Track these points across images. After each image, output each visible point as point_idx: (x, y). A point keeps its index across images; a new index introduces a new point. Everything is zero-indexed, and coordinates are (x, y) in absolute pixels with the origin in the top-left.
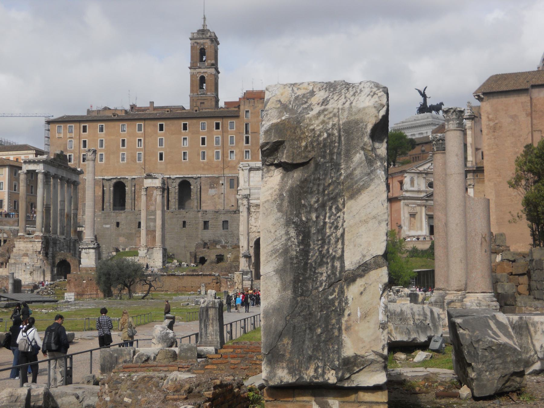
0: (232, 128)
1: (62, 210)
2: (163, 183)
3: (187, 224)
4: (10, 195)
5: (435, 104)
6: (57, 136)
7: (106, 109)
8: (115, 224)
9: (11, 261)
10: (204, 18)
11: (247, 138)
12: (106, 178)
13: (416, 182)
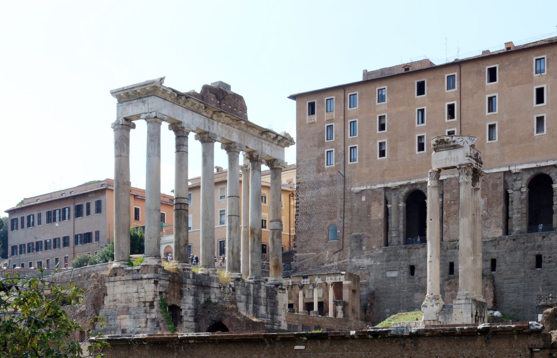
3: (545, 260)
6: (308, 122)
8: (408, 269)
12: (390, 185)
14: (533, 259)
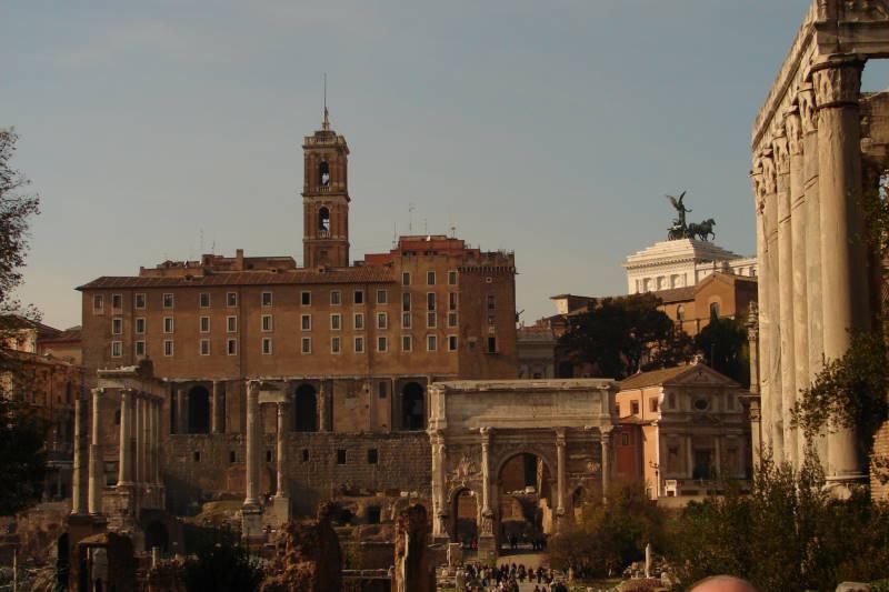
5: (698, 222)
7: (168, 265)
10: (326, 112)
12: (177, 380)
13: (677, 402)
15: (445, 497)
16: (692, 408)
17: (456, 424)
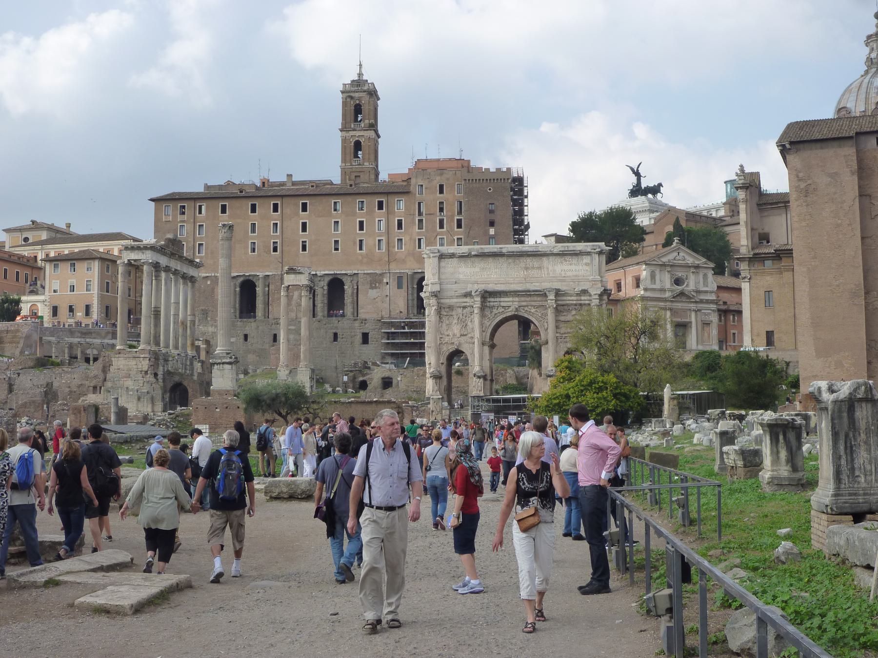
0: (400, 206)
1: (176, 315)
2: (311, 280)
4: (101, 298)
5: (651, 185)
8: (243, 337)
9: (109, 384)
10: (361, 65)
11: (420, 221)
13: (657, 277)
14: (332, 336)
15: (438, 359)
16: (672, 285)
17: (449, 286)
